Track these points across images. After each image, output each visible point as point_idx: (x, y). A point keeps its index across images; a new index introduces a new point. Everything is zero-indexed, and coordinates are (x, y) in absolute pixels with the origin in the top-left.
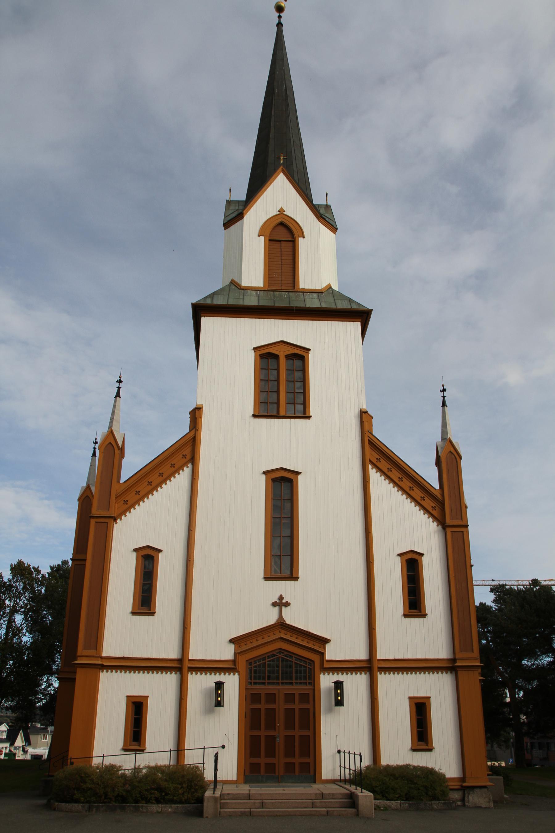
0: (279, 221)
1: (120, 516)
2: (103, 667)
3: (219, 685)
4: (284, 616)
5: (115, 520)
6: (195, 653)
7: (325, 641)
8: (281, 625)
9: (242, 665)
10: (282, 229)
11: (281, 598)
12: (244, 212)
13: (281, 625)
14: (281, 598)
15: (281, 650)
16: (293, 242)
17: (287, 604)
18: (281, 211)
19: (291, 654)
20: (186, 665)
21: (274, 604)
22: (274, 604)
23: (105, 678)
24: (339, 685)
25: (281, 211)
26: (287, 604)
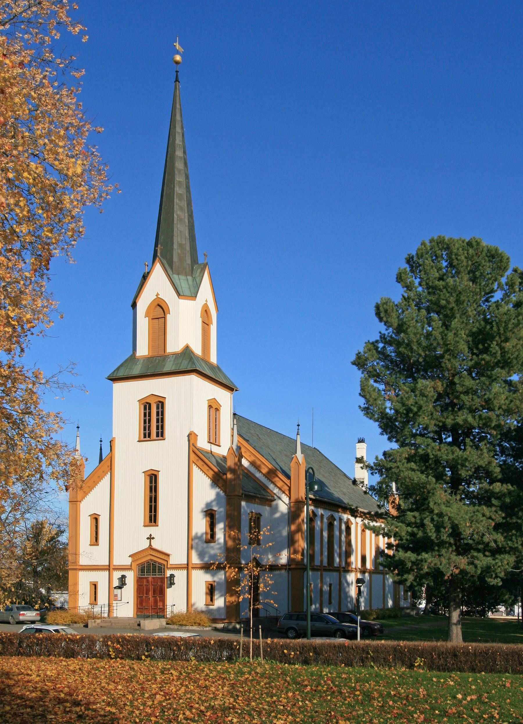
0: (156, 304)
1: (82, 500)
2: (80, 569)
3: (124, 577)
4: (152, 544)
5: (80, 502)
6: (116, 562)
7: (168, 555)
8: (150, 548)
9: (134, 566)
10: (159, 307)
11: (151, 535)
12: (137, 301)
13: (150, 548)
14: (151, 535)
15: (151, 560)
16: (165, 318)
17: (153, 538)
18: (158, 295)
19: (155, 562)
20: (112, 567)
21: (148, 538)
22: (148, 538)
23: (82, 574)
24: (172, 576)
25: (158, 295)
26: (153, 538)
